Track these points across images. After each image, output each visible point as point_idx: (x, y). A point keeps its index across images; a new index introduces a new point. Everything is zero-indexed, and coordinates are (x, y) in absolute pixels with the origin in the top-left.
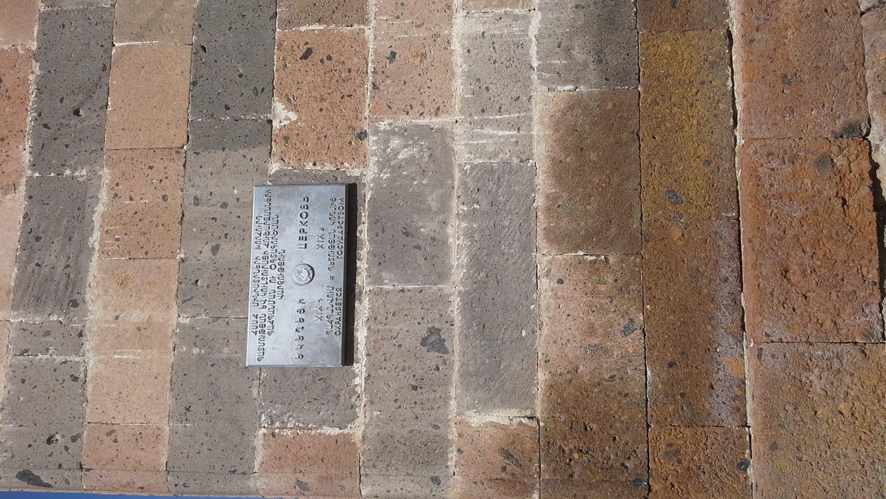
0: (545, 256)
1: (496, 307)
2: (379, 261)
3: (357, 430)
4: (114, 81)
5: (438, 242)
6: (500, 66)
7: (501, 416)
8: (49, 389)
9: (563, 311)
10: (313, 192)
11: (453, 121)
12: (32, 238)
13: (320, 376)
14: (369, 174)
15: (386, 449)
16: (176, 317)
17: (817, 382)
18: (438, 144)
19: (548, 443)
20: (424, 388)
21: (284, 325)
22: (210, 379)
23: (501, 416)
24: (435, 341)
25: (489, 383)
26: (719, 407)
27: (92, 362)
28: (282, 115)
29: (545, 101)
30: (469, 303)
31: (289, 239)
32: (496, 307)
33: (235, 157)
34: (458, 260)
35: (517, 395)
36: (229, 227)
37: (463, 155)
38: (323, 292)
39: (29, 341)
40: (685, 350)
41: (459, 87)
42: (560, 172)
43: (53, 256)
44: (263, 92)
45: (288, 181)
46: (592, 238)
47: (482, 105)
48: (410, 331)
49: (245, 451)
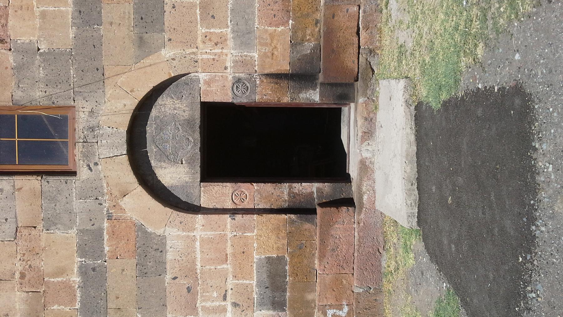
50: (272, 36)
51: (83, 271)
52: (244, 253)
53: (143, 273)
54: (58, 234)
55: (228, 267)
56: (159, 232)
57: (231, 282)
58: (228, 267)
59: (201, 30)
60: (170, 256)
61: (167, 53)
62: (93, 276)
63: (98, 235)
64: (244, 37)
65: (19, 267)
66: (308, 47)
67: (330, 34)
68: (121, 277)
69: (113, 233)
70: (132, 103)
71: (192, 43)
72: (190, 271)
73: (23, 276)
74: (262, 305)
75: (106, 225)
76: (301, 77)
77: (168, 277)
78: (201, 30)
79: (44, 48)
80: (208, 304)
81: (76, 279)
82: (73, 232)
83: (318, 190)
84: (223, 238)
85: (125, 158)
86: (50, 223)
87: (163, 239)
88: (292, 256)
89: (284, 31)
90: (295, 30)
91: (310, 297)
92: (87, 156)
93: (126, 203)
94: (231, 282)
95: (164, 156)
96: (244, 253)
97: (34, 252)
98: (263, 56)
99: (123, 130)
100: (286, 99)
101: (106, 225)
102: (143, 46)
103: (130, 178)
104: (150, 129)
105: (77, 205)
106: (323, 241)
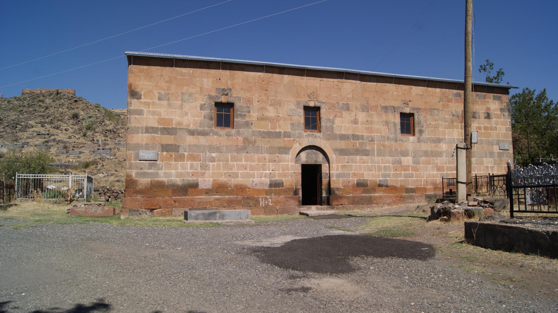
0: (150, 179)
1: (144, 175)
2: (149, 163)
3: (133, 161)
4: (169, 136)
5: (151, 169)
6: (169, 175)
7: (134, 175)
8: (136, 130)
9: (144, 181)
10: (156, 157)
11: (164, 171)
12: (152, 128)
13: (138, 158)
14: (158, 162)
15: (131, 164)
16: (144, 143)
17: (137, 203)
18: (161, 169)
19: (132, 179)
20: (137, 168)
21: (144, 154)
22: (138, 147)
23: (134, 175)
24: (141, 169)
25: (137, 174)
26: (135, 195)
27: (140, 135)
28: (165, 153)
29: (165, 180)
30: (145, 172)
31: (152, 154)
32: (144, 175)
33: (161, 149)
34: (149, 171)
35: (136, 177)
36: (153, 148)
37: (160, 171)
38: (146, 158)
39: (142, 128)
40: (140, 192)
41: (167, 171)
42: (158, 181)
43: (150, 130)
44: (167, 152)
45: (158, 154)
46: (151, 184)
47: (165, 173)
48: (142, 166)
49: (131, 150)
50: (339, 183)
51: (280, 132)
52: (285, 176)
53: (279, 148)
54: (289, 126)
55: (281, 171)
56: (290, 153)
57: (277, 172)
58: (281, 171)
59: (340, 165)
60: (284, 155)
61: (334, 156)
62: (278, 135)
63: (289, 137)
64: (338, 176)
65: (281, 115)
66: (337, 192)
67: (341, 197)
68: (279, 142)
69: (290, 141)
70: (322, 147)
71: (337, 163)
72: (280, 161)
73: (278, 116)
74: (271, 181)
75: (292, 139)
76: (330, 190)
77: (278, 155)
78: (340, 165)
79: (334, 126)
80: (271, 166)
81: (278, 130)
82: (290, 130)
83: (299, 197)
84: (289, 170)
85: (309, 145)
86: (292, 124)
87: (288, 154)
88: (284, 189)
89: (341, 186)
90: (341, 189)
91: (273, 194)
92: (309, 135)
93: (298, 144)
94: (277, 172)
95: (308, 154)
96: (285, 176)
97: (285, 120)
98: (334, 181)
99: (316, 145)
100: (323, 187)
101: (292, 139)
102: (335, 150)
103: (304, 146)
104: (314, 151)
105: (297, 132)
106: (290, 197)
